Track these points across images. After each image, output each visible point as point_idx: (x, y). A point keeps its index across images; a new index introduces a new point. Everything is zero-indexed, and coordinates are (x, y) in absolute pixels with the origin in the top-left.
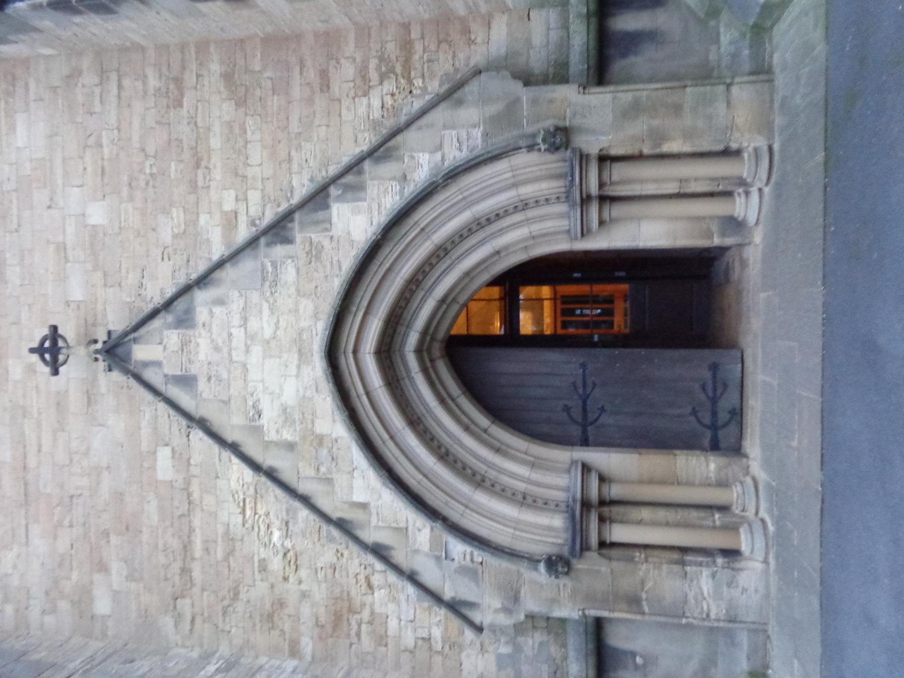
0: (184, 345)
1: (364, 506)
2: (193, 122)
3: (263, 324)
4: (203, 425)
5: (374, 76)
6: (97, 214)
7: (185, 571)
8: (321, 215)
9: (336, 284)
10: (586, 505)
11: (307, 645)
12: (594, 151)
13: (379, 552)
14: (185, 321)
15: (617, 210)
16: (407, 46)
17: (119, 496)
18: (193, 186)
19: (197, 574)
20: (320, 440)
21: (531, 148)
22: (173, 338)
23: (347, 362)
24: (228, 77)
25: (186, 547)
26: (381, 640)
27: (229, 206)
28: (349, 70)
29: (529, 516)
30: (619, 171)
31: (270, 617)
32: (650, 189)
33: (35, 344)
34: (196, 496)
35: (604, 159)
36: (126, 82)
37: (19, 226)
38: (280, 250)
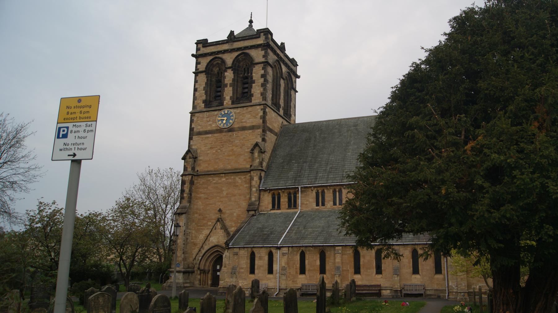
0: (219, 228)
3: (220, 238)
4: (211, 231)
6: (235, 214)
10: (205, 271)
11: (192, 241)
13: (200, 250)
14: (221, 229)
17: (206, 217)
22: (220, 227)
23: (216, 247)
26: (193, 249)
29: (203, 266)
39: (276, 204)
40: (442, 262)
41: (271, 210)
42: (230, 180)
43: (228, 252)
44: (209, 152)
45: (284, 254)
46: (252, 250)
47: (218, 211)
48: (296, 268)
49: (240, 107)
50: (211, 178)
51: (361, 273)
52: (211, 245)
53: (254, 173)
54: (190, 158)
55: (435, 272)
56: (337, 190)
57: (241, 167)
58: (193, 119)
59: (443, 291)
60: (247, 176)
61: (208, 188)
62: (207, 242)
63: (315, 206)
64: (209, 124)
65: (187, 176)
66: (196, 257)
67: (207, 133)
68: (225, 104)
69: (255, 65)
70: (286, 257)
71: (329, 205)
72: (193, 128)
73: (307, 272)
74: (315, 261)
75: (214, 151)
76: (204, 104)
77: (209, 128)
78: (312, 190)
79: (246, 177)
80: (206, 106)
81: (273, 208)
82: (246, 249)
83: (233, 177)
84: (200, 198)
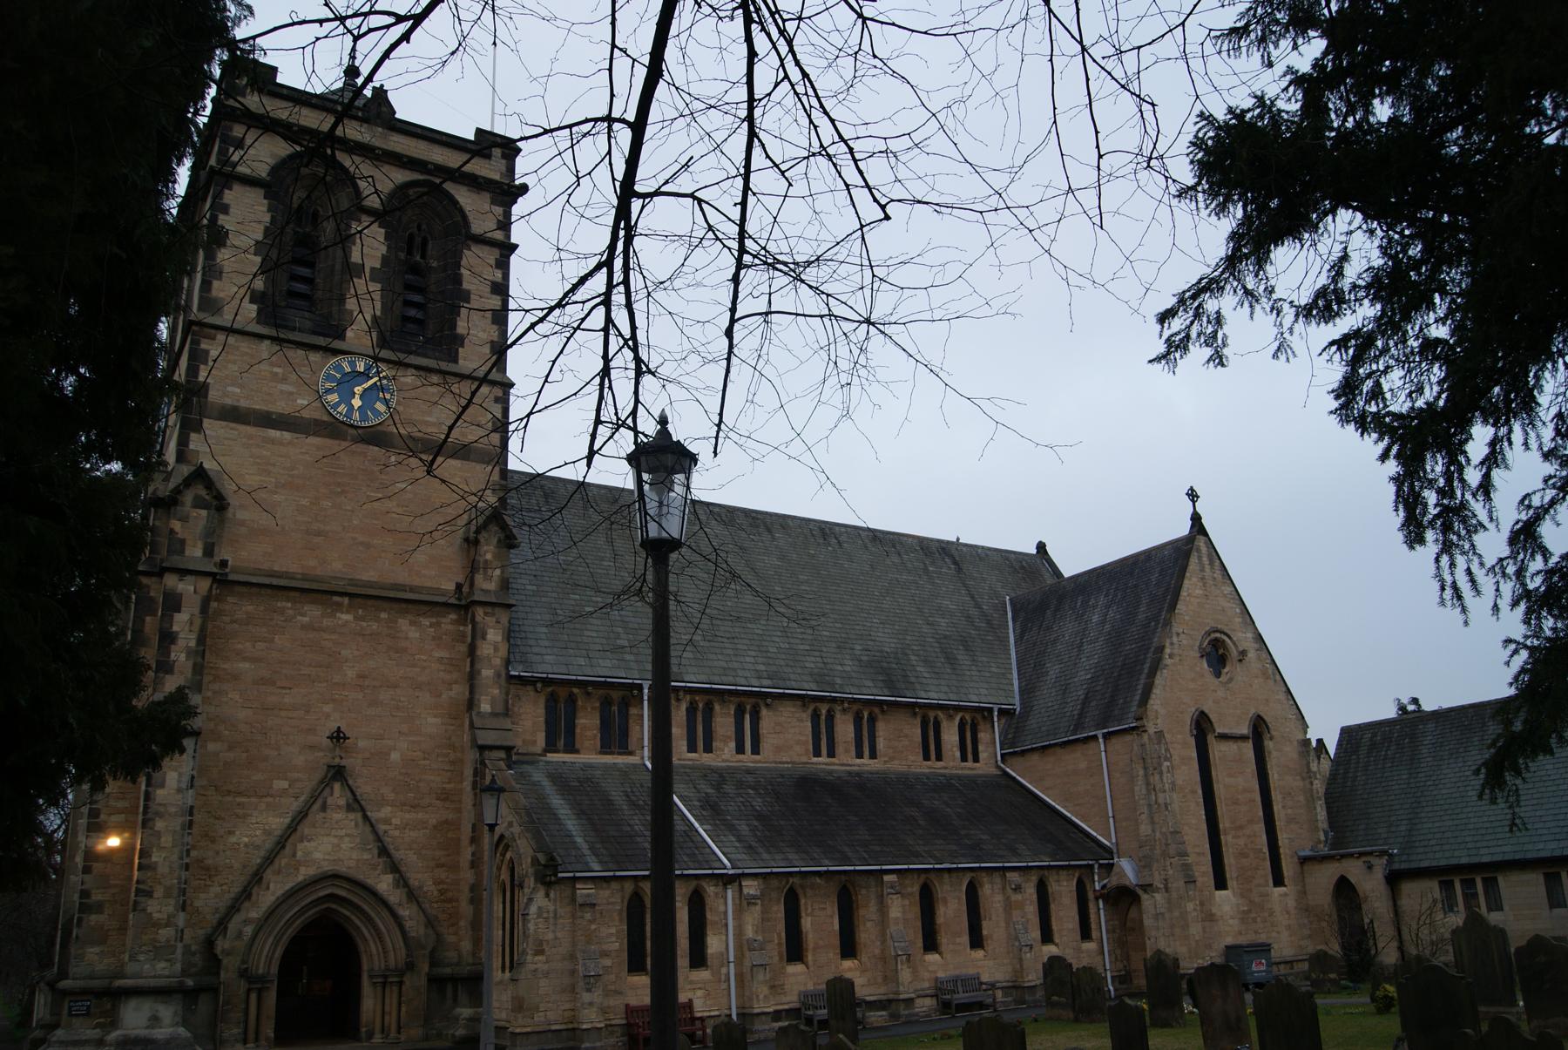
1: (268, 888)
2: (430, 805)
5: (441, 886)
6: (395, 756)
7: (229, 792)
8: (389, 870)
9: (361, 877)
12: (405, 979)
14: (349, 808)
15: (379, 989)
16: (450, 901)
18: (404, 804)
19: (229, 799)
20: (297, 869)
21: (407, 955)
22: (342, 802)
24: (446, 822)
25: (240, 794)
27: (394, 821)
28: (443, 876)
30: (395, 989)
31: (206, 835)
32: (387, 1001)
33: (342, 729)
34: (265, 800)
35: (401, 983)
36: (449, 774)
37: (393, 716)
38: (376, 852)
39: (560, 733)
41: (545, 751)
42: (375, 626)
43: (547, 895)
44: (277, 497)
45: (751, 901)
46: (637, 886)
47: (331, 738)
48: (779, 944)
49: (417, 368)
50: (289, 605)
51: (943, 948)
52: (304, 873)
53: (486, 614)
54: (199, 503)
56: (748, 707)
57: (417, 582)
58: (207, 352)
60: (444, 620)
61: (272, 641)
62: (282, 861)
63: (685, 748)
64: (282, 392)
65: (189, 578)
66: (233, 926)
67: (267, 420)
68: (349, 334)
69: (470, 243)
70: (758, 908)
71: (726, 750)
72: (205, 387)
73: (810, 958)
74: (832, 917)
75: (304, 502)
76: (255, 307)
77: (280, 407)
78: (678, 700)
79: (438, 624)
80: (262, 317)
81: (551, 746)
82: (615, 885)
83: (384, 615)
84: (236, 677)
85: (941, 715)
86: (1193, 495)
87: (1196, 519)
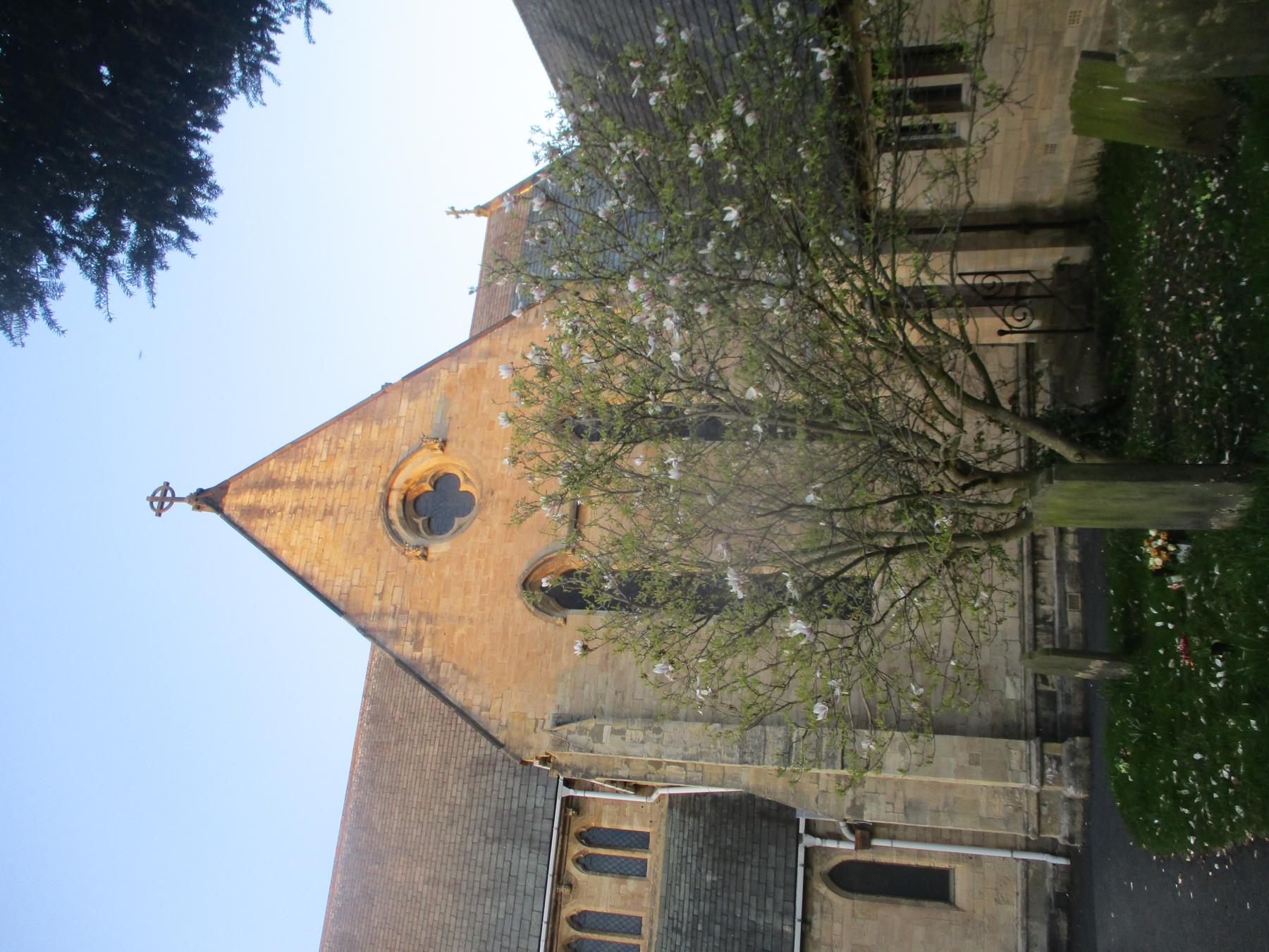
40: (894, 860)
55: (941, 904)
59: (1032, 875)
85: (568, 910)
86: (162, 499)
87: (209, 499)
